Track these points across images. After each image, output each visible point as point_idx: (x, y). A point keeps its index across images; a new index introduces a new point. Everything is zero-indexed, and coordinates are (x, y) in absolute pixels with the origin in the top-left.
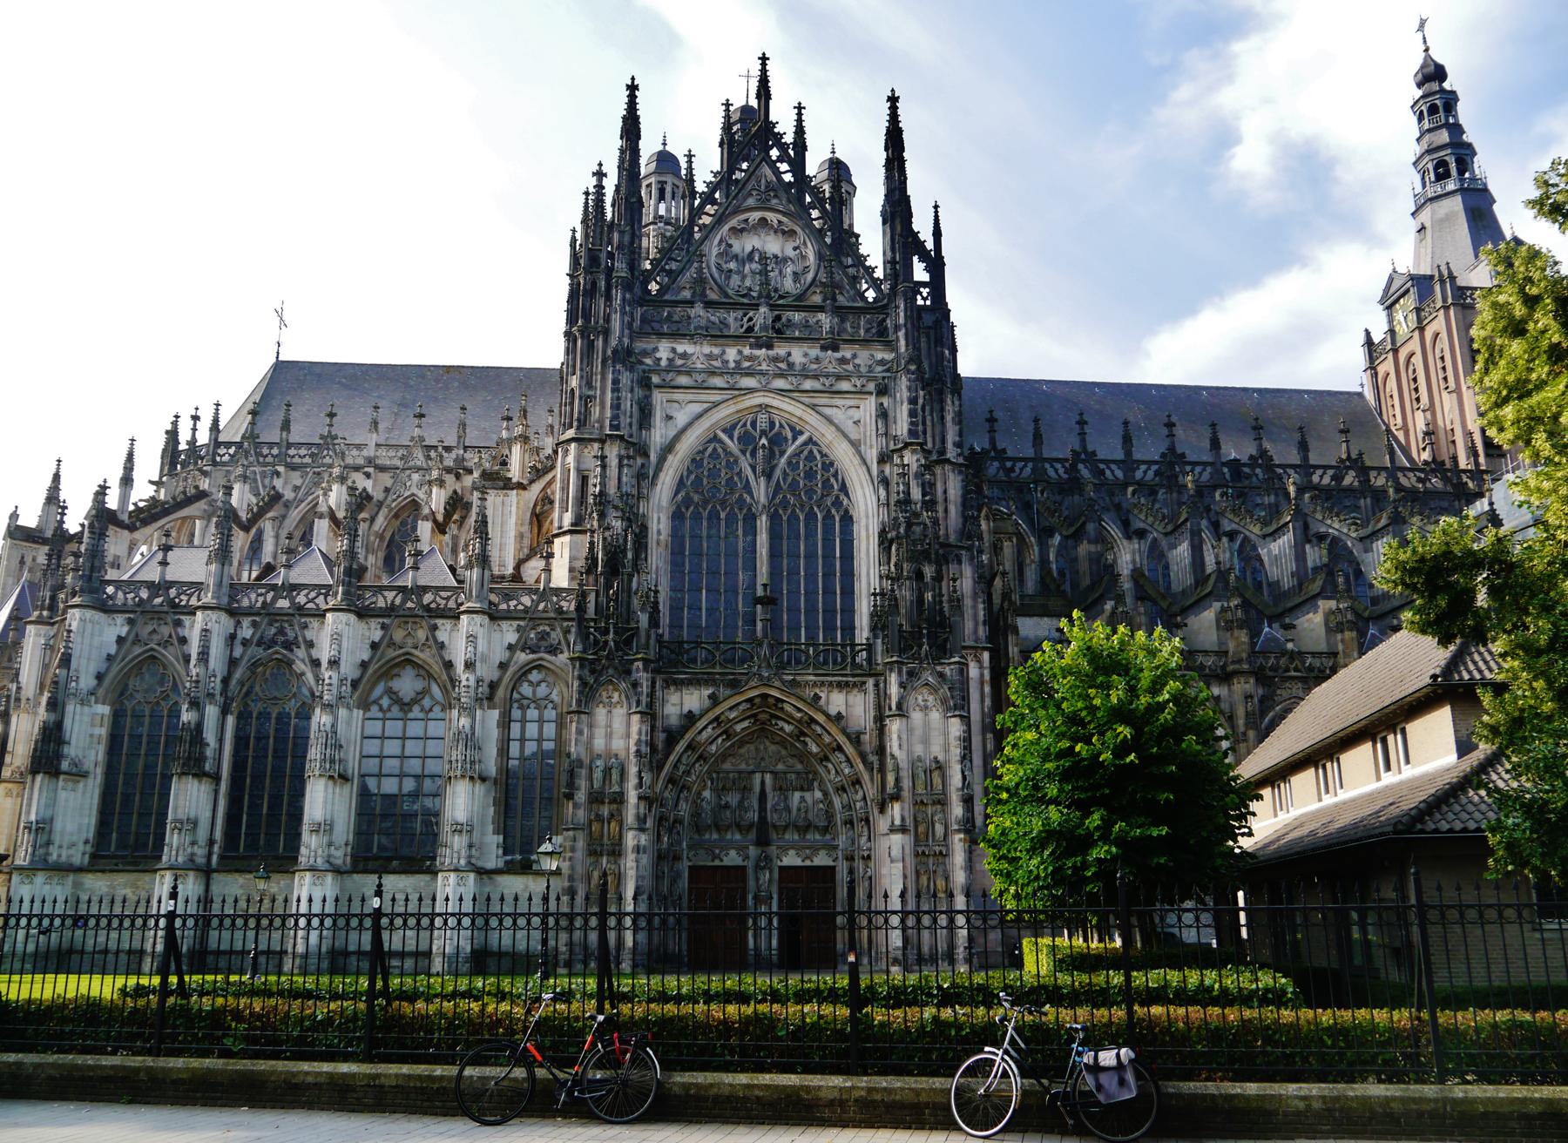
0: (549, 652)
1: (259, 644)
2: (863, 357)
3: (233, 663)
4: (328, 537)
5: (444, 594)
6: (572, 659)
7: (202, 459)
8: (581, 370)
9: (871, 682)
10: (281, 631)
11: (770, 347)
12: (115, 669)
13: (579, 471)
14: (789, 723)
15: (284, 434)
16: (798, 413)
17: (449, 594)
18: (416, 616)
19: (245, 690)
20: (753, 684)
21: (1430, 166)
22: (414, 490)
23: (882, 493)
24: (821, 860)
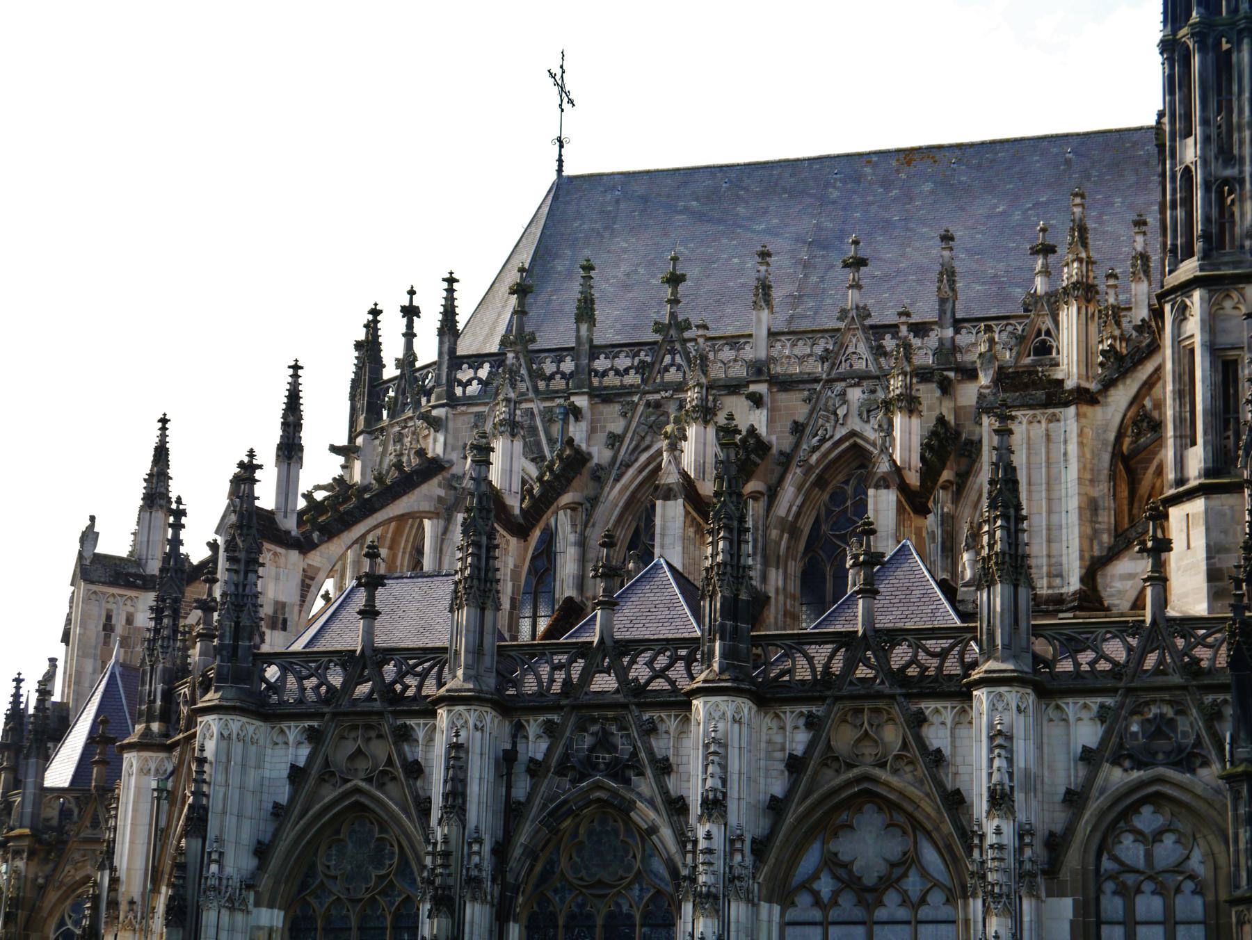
1: (561, 771)
3: (512, 812)
4: (684, 538)
5: (932, 644)
6: (1229, 778)
7: (428, 394)
8: (1205, 122)
10: (604, 742)
12: (288, 836)
13: (1213, 349)
15: (584, 328)
17: (945, 643)
18: (879, 696)
19: (539, 868)
22: (855, 424)
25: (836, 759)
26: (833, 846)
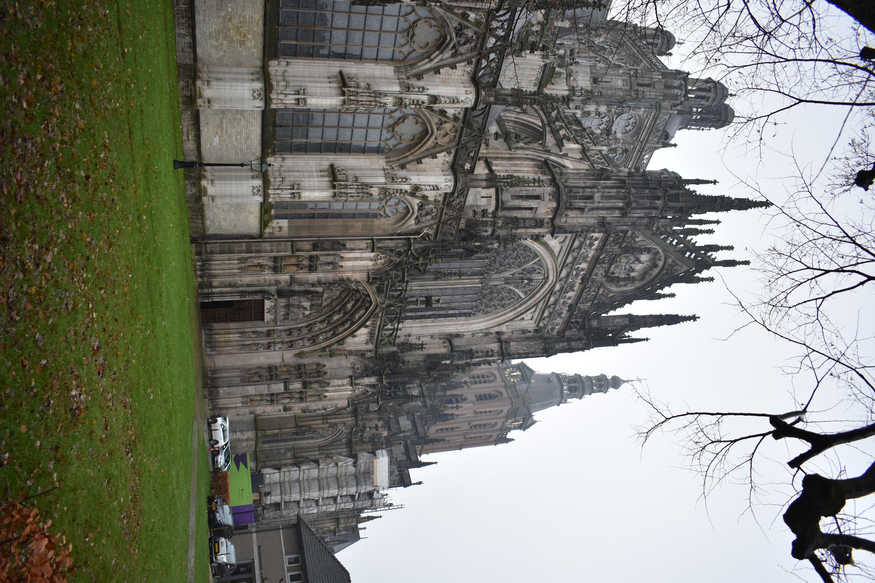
0: (417, 218)
2: (559, 320)
9: (371, 346)
11: (580, 283)
14: (353, 306)
16: (537, 296)
20: (379, 300)
21: (576, 384)
23: (481, 334)
24: (268, 317)
25: (441, 124)
26: (411, 118)
